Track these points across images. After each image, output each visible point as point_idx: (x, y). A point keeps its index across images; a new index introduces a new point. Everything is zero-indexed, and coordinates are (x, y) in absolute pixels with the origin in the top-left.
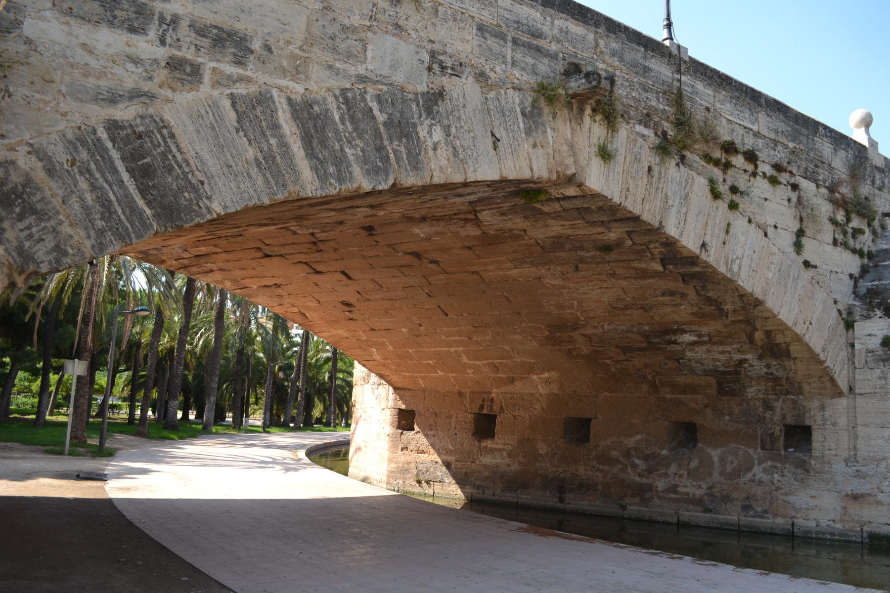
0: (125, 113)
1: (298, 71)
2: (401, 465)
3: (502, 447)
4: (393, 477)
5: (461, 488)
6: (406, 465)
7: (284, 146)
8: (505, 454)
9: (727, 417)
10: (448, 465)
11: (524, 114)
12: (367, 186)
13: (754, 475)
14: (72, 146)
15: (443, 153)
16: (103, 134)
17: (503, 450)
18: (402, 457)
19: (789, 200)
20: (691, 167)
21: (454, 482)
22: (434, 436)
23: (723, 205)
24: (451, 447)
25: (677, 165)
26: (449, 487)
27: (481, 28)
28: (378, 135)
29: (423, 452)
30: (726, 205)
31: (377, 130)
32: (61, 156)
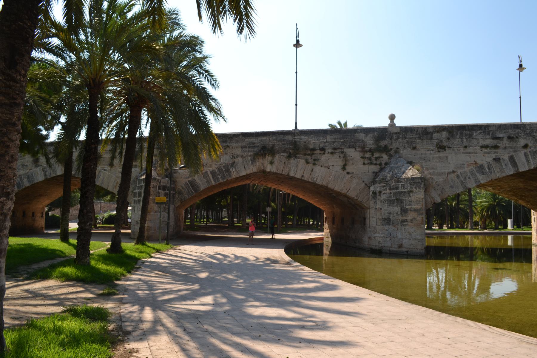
0: (190, 179)
1: (211, 166)
7: (210, 178)
11: (251, 161)
12: (222, 181)
14: (185, 185)
15: (235, 173)
16: (188, 182)
19: (340, 157)
20: (299, 158)
23: (310, 165)
25: (294, 159)
27: (242, 147)
28: (224, 173)
30: (312, 165)
31: (223, 172)
32: (184, 186)
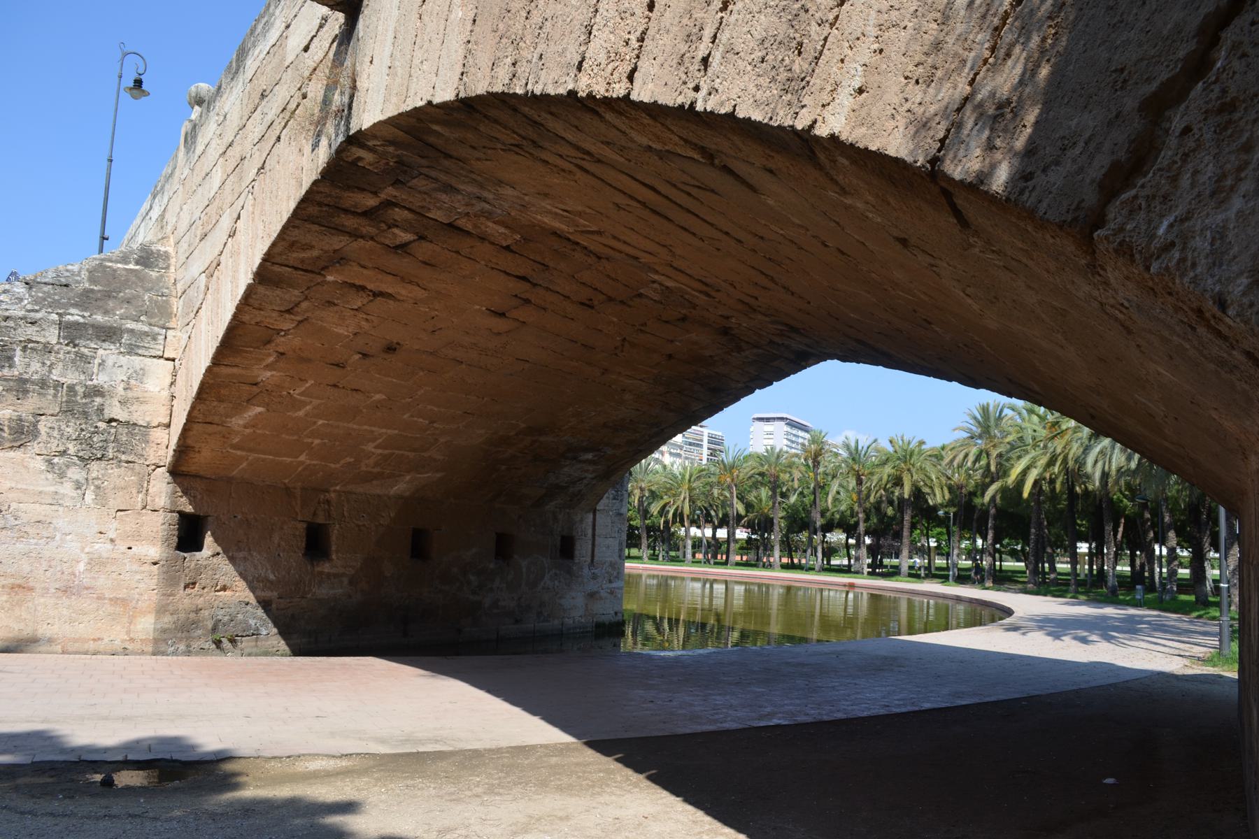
2: (182, 616)
3: (341, 570)
4: (165, 641)
5: (285, 639)
6: (192, 616)
8: (346, 580)
9: (533, 529)
10: (265, 604)
13: (545, 584)
17: (343, 575)
18: (185, 600)
21: (275, 630)
22: (245, 559)
24: (272, 577)
26: (267, 640)
29: (224, 588)
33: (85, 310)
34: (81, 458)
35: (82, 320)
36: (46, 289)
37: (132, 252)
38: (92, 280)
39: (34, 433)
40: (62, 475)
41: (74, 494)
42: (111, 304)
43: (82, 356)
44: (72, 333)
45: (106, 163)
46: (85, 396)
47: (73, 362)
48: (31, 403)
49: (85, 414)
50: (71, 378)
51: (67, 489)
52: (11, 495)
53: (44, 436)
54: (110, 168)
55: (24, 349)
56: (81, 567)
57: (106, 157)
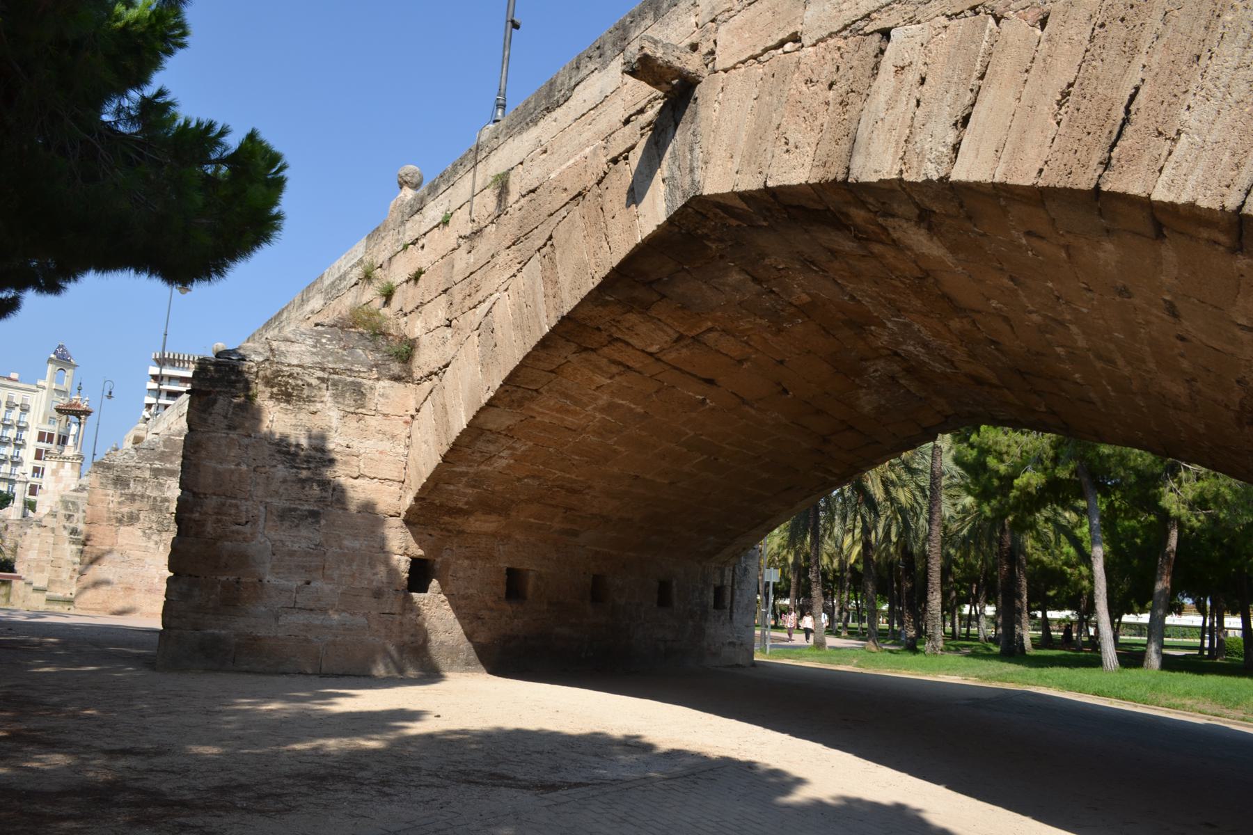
33: (162, 461)
34: (158, 531)
35: (160, 467)
36: (144, 451)
37: (183, 430)
38: (165, 446)
39: (138, 519)
40: (149, 538)
41: (154, 546)
42: (173, 458)
43: (160, 484)
44: (156, 473)
45: (163, 336)
46: (161, 502)
47: (156, 486)
48: (137, 505)
49: (161, 511)
50: (155, 494)
51: (152, 544)
52: (127, 547)
53: (142, 521)
54: (165, 339)
55: (135, 480)
56: (157, 580)
57: (163, 332)
